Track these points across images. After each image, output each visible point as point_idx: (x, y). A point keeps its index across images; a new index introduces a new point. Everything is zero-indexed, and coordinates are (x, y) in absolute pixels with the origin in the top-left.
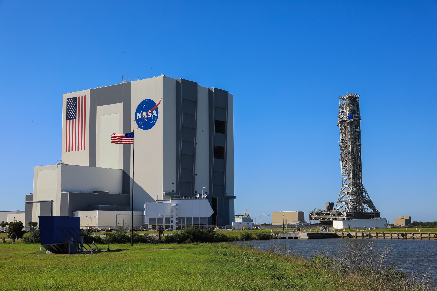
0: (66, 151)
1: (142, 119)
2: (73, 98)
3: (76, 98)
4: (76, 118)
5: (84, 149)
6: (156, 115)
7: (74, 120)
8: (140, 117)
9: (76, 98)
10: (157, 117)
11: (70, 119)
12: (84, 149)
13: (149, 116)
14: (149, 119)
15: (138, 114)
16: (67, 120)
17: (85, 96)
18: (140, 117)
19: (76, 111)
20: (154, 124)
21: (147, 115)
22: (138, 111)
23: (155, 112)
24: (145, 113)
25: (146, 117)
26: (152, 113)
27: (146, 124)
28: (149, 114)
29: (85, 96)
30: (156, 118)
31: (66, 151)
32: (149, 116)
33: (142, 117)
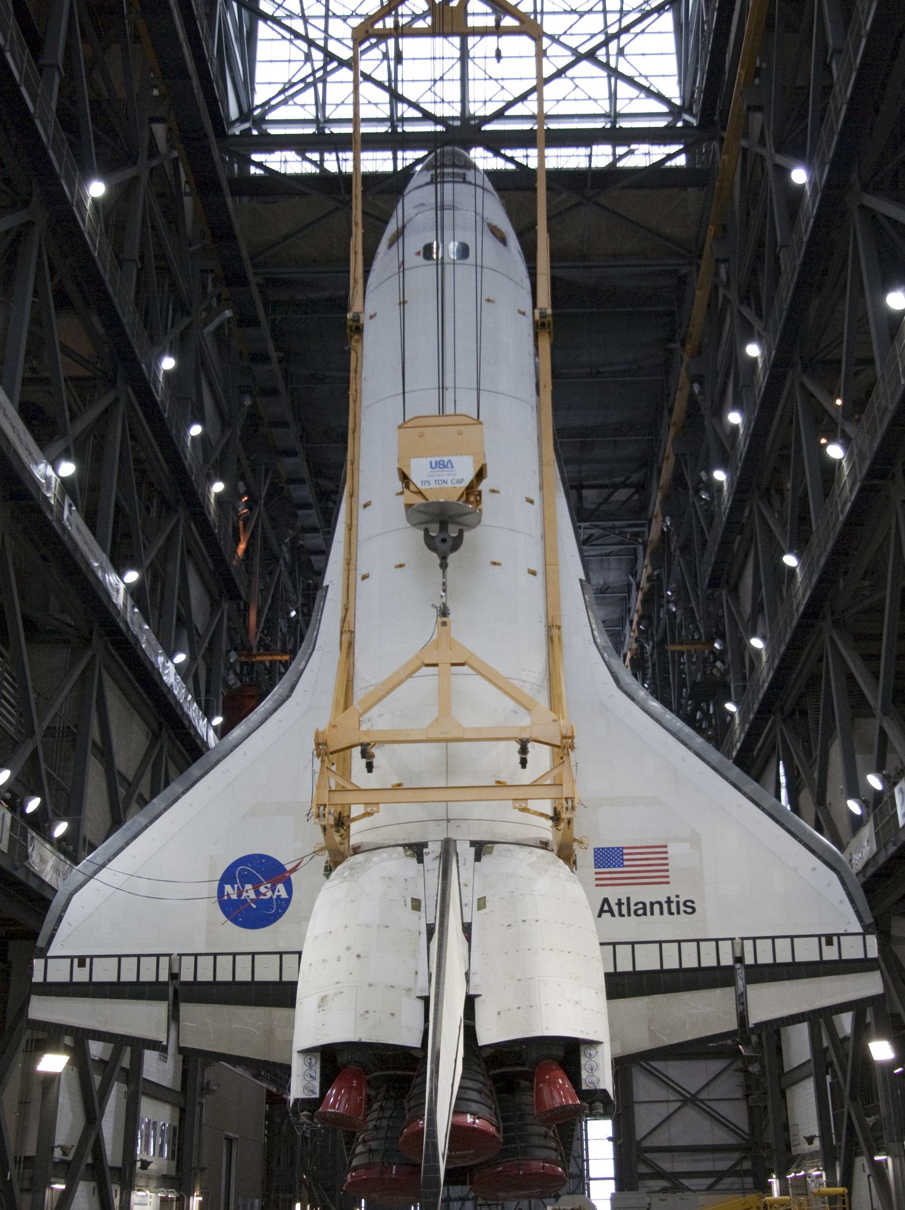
1: (240, 902)
6: (284, 895)
10: (288, 901)
13: (265, 895)
20: (277, 916)
21: (258, 893)
22: (228, 877)
23: (281, 887)
25: (252, 895)
28: (262, 889)
30: (283, 905)
32: (265, 895)
33: (239, 895)
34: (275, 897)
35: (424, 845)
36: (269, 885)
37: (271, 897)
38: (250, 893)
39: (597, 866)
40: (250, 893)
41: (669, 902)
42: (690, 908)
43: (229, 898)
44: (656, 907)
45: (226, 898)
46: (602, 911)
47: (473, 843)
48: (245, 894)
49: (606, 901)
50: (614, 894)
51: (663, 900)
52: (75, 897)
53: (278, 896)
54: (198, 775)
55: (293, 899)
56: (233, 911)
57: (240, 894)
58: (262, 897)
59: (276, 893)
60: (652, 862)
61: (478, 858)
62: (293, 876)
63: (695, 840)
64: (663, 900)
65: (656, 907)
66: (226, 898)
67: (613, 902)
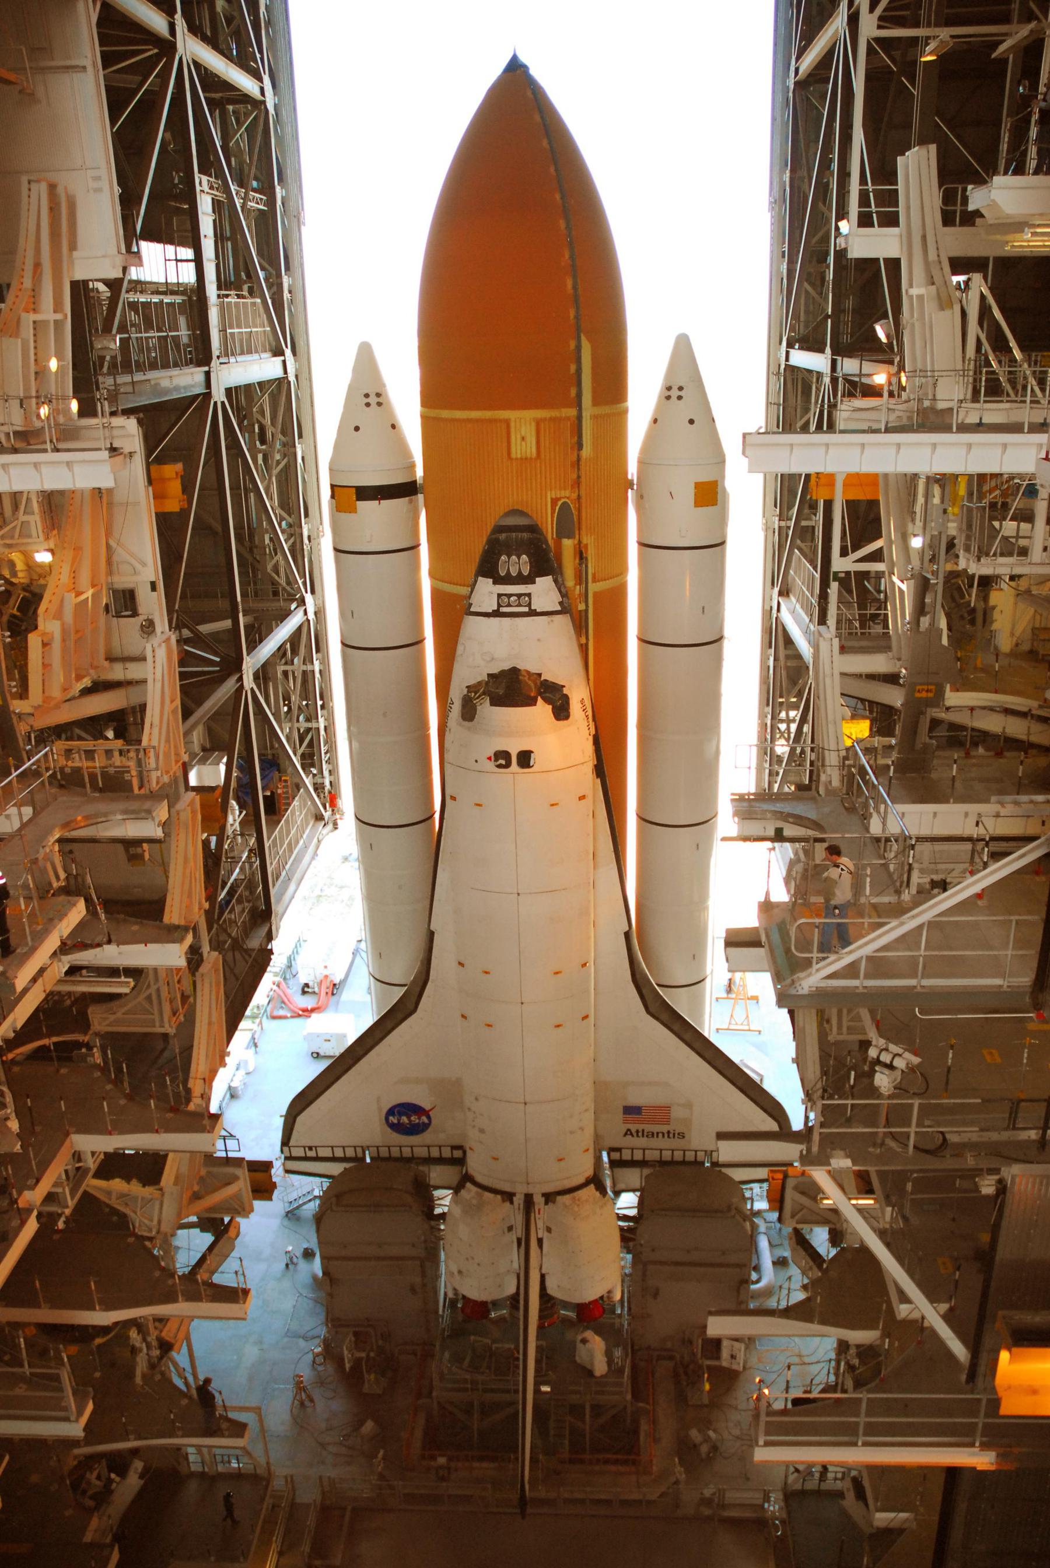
8: (396, 1121)
10: (429, 1124)
20: (423, 1131)
22: (391, 1112)
26: (419, 1118)
35: (514, 1194)
38: (404, 1119)
39: (624, 1113)
40: (404, 1119)
41: (669, 1132)
42: (682, 1136)
44: (660, 1135)
46: (626, 1134)
47: (543, 1195)
49: (629, 1130)
50: (634, 1128)
51: (665, 1131)
52: (299, 1119)
54: (361, 1053)
55: (433, 1122)
57: (399, 1120)
60: (662, 1113)
61: (546, 1203)
63: (689, 1105)
64: (665, 1131)
65: (660, 1135)
67: (633, 1131)
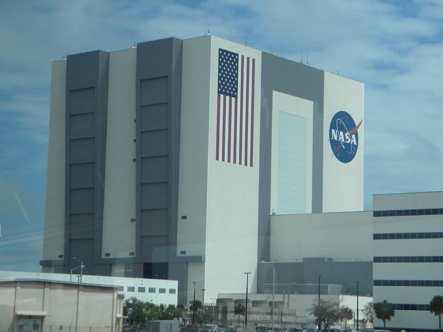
0: (217, 159)
2: (231, 53)
3: (238, 55)
4: (236, 97)
5: (251, 165)
6: (355, 143)
7: (233, 99)
8: (336, 139)
9: (237, 55)
10: (357, 146)
11: (225, 94)
12: (251, 165)
13: (348, 141)
14: (348, 146)
15: (333, 131)
16: (219, 93)
17: (254, 60)
18: (336, 139)
19: (237, 83)
20: (353, 156)
21: (345, 137)
23: (354, 136)
24: (341, 133)
25: (343, 140)
27: (345, 153)
29: (254, 60)
31: (217, 159)
32: (348, 141)
33: (338, 138)
34: (351, 143)
36: (349, 134)
37: (350, 142)
43: (334, 138)
45: (332, 138)
48: (340, 138)
53: (353, 143)
56: (336, 149)
58: (347, 142)
59: (352, 141)
62: (358, 130)
66: (332, 138)
